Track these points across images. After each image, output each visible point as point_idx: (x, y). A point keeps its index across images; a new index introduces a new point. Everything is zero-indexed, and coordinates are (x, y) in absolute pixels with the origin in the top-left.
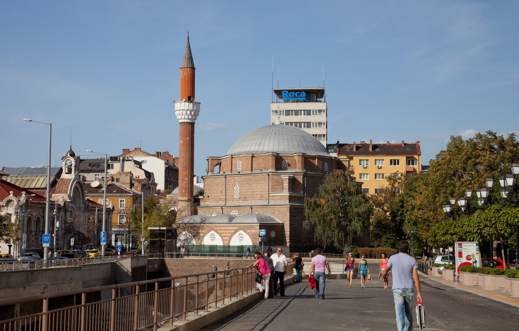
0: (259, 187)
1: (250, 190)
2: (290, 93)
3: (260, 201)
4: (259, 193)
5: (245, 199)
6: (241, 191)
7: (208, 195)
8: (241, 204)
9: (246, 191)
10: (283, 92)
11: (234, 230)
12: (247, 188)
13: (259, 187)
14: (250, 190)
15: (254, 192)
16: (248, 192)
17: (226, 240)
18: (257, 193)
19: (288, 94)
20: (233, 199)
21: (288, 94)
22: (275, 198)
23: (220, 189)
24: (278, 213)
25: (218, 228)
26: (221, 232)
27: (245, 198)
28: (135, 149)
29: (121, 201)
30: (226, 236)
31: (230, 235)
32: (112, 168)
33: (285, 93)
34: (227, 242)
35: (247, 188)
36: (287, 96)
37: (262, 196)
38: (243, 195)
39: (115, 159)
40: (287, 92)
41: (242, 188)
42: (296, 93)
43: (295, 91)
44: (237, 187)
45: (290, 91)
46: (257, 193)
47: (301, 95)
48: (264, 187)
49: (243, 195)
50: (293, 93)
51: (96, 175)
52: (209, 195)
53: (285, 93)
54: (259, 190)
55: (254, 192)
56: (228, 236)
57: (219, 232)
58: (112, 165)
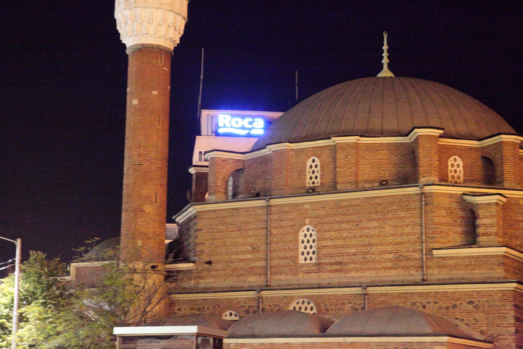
0: (388, 230)
1: (354, 241)
3: (392, 273)
4: (389, 248)
5: (340, 266)
6: (324, 243)
7: (207, 259)
8: (324, 282)
12: (345, 234)
13: (388, 230)
14: (354, 241)
15: (371, 245)
16: (349, 246)
18: (380, 248)
19: (230, 122)
22: (451, 262)
23: (251, 240)
24: (471, 307)
27: (340, 263)
35: (345, 234)
38: (331, 256)
41: (328, 235)
44: (306, 234)
46: (380, 248)
47: (255, 125)
48: (408, 230)
49: (331, 256)
52: (212, 259)
54: (390, 239)
55: (371, 245)
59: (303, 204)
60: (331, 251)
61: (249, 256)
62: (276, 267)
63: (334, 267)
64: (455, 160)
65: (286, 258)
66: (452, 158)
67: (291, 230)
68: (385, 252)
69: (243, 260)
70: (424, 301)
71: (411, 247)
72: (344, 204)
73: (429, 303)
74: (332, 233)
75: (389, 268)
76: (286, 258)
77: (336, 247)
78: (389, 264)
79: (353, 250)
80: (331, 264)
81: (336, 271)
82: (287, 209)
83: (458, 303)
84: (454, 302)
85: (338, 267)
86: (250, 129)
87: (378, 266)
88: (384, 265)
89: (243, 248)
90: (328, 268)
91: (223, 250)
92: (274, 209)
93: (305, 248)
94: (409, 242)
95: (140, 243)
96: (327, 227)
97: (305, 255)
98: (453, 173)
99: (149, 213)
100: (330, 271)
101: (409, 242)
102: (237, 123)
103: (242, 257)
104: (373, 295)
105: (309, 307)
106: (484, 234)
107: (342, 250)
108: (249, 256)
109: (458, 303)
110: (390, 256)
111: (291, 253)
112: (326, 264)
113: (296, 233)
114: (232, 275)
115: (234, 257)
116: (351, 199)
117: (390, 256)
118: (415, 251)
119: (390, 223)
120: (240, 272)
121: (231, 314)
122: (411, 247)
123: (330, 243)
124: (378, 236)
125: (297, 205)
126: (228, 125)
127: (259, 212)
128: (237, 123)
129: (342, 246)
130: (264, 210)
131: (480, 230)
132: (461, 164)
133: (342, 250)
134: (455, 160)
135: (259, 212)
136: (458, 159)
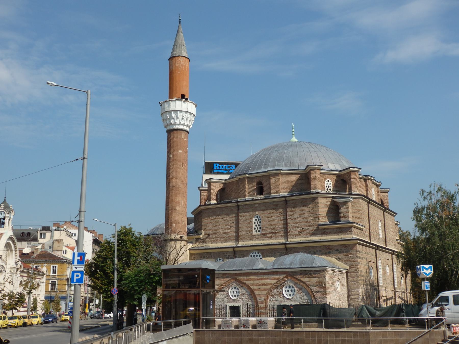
2: (221, 166)
5: (273, 235)
9: (273, 223)
10: (215, 165)
11: (275, 279)
12: (275, 218)
13: (297, 216)
17: (260, 296)
19: (219, 167)
20: (252, 237)
21: (219, 167)
22: (327, 231)
23: (229, 223)
25: (245, 278)
26: (252, 282)
27: (273, 233)
28: (65, 222)
29: (53, 267)
30: (259, 289)
31: (268, 287)
32: (45, 237)
33: (216, 165)
34: (263, 299)
35: (275, 218)
36: (218, 168)
37: (302, 229)
38: (269, 229)
39: (46, 229)
40: (218, 165)
41: (267, 219)
42: (227, 166)
43: (226, 164)
45: (220, 164)
47: (231, 168)
49: (269, 229)
50: (224, 166)
51: (28, 243)
52: (210, 232)
53: (216, 165)
54: (298, 220)
56: (265, 290)
57: (247, 282)
58: (45, 234)
59: (254, 204)
60: (269, 227)
61: (228, 231)
62: (241, 236)
63: (271, 235)
64: (328, 181)
65: (247, 231)
66: (327, 180)
67: (249, 217)
68: (295, 227)
69: (225, 233)
70: (315, 250)
71: (308, 224)
72: (275, 204)
73: (317, 251)
74: (269, 218)
75: (298, 235)
76: (247, 231)
77: (271, 225)
78: (297, 233)
79: (280, 227)
80: (270, 233)
81: (272, 237)
82: (247, 207)
83: (331, 251)
84: (329, 251)
85: (272, 235)
86: (229, 170)
87: (292, 234)
88: (295, 233)
89: (225, 227)
90: (268, 235)
91: (215, 228)
92: (240, 207)
93: (256, 226)
94: (307, 222)
95: (174, 225)
96: (267, 215)
97: (256, 229)
98: (327, 188)
99: (178, 211)
100: (268, 237)
101: (307, 222)
102: (222, 167)
103: (225, 231)
104: (290, 248)
105: (258, 255)
106: (343, 217)
107: (274, 227)
108: (228, 231)
109: (331, 251)
110: (298, 229)
111: (249, 229)
112: (267, 234)
113: (251, 219)
114: (220, 240)
115: (222, 231)
116: (278, 201)
117: (298, 229)
118: (310, 226)
119: (298, 212)
120: (224, 239)
121: (220, 260)
122: (308, 224)
123: (268, 223)
124: (292, 219)
125: (251, 205)
126: (218, 168)
127: (233, 209)
128: (222, 167)
129: (274, 225)
130: (236, 208)
131: (342, 215)
132: (331, 183)
133: (274, 227)
134: (328, 181)
135: (233, 209)
136: (330, 180)
